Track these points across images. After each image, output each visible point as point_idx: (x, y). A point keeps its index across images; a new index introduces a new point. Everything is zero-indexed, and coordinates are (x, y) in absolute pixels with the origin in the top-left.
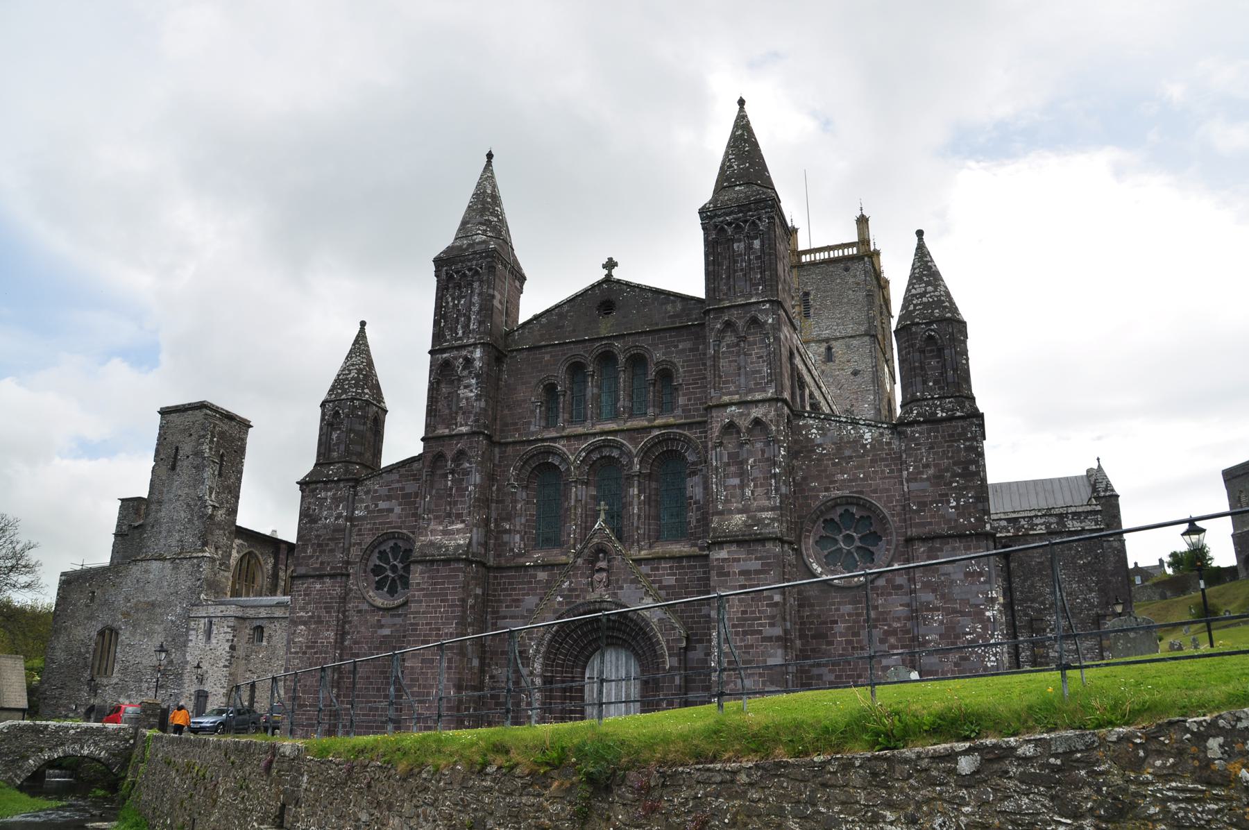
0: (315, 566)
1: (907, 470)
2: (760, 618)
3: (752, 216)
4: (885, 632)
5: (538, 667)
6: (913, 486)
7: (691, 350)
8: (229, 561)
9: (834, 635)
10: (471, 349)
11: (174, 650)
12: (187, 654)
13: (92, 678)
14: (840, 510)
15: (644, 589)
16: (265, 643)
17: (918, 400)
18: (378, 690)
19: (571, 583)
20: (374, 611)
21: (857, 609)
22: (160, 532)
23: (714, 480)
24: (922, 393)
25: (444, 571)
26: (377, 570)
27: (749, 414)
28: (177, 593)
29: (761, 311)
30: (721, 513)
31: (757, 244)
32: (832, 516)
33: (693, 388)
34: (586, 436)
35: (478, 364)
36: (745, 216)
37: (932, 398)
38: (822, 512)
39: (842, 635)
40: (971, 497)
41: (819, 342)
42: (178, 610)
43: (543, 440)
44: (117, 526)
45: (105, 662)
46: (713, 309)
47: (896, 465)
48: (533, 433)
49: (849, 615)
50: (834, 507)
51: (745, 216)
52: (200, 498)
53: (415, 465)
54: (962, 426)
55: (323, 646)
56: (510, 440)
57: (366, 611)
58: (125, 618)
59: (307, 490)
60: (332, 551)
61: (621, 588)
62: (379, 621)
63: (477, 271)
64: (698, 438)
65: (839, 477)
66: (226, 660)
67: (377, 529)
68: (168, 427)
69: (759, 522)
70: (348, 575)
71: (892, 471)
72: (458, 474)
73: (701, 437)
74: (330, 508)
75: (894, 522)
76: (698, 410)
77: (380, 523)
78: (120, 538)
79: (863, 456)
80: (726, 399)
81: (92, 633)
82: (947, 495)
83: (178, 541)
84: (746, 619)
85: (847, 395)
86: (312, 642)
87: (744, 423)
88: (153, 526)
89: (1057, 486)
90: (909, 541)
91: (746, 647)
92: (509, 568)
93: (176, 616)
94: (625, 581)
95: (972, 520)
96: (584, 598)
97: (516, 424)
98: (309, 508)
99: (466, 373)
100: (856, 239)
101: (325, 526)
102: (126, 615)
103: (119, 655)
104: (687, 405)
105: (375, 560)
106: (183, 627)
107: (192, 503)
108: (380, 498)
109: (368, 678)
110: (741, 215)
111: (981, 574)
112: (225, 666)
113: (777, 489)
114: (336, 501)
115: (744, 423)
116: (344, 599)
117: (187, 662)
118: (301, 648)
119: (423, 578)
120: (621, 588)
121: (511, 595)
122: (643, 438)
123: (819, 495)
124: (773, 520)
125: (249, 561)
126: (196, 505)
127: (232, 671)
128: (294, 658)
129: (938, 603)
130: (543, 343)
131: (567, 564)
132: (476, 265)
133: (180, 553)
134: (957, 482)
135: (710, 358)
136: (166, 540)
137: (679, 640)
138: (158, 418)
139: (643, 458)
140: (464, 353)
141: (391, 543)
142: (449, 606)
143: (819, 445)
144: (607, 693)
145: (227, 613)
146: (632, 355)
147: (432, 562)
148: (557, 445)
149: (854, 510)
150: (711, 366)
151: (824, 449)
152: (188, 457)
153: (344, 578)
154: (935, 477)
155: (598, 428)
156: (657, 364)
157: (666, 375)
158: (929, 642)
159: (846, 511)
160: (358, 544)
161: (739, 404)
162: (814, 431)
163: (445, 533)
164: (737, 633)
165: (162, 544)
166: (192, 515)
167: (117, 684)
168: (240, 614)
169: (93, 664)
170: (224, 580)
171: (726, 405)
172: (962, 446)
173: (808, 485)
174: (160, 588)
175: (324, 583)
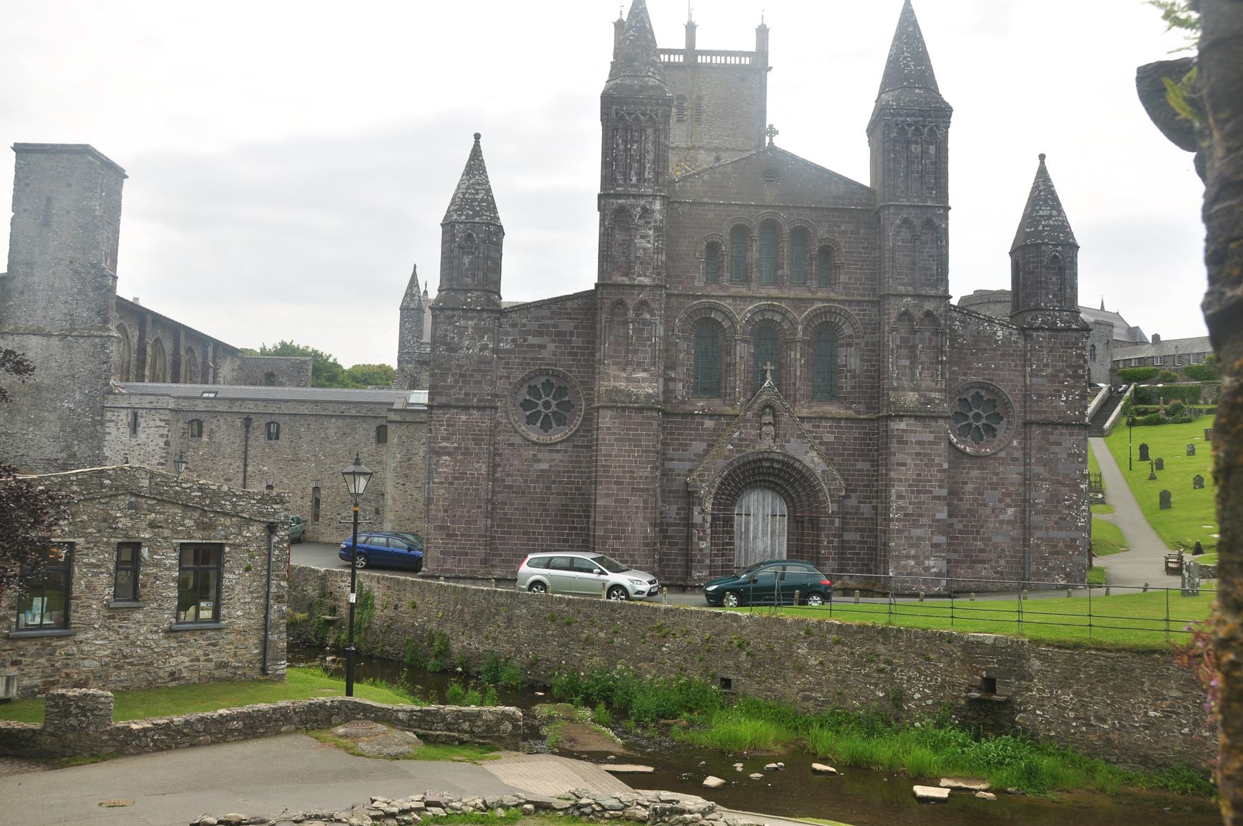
0: (458, 396)
1: (1031, 366)
2: (931, 481)
3: (931, 122)
4: (1003, 493)
5: (708, 506)
6: (1035, 380)
7: (852, 233)
9: (964, 493)
10: (650, 199)
12: (105, 449)
14: (972, 392)
15: (809, 445)
16: (205, 439)
17: (1043, 309)
18: (537, 521)
19: (741, 433)
20: (528, 445)
21: (982, 474)
22: (35, 301)
23: (890, 360)
24: (1046, 304)
25: (637, 418)
26: (526, 405)
27: (922, 307)
28: (73, 376)
29: (936, 215)
30: (896, 389)
31: (932, 149)
32: (966, 397)
33: (854, 269)
34: (753, 299)
35: (658, 216)
36: (924, 120)
37: (1054, 310)
38: (959, 392)
39: (970, 493)
40: (1077, 395)
41: (709, 150)
42: (78, 396)
43: (708, 297)
46: (894, 205)
47: (1020, 360)
48: (698, 288)
49: (976, 478)
50: (968, 389)
51: (924, 120)
53: (569, 304)
54: (1076, 337)
55: (473, 478)
56: (676, 292)
57: (519, 445)
59: (442, 316)
60: (479, 382)
61: (789, 441)
62: (534, 455)
63: (651, 116)
64: (857, 315)
65: (975, 365)
66: (161, 457)
67: (529, 364)
69: (931, 401)
70: (496, 408)
71: (1016, 365)
72: (638, 323)
73: (860, 315)
74: (472, 338)
75: (1017, 407)
76: (857, 289)
77: (531, 359)
79: (995, 350)
80: (902, 289)
82: (1059, 391)
84: (920, 481)
86: (459, 473)
87: (918, 314)
88: (22, 293)
90: (1027, 424)
91: (919, 503)
92: (677, 415)
93: (75, 403)
94: (792, 435)
96: (754, 447)
97: (680, 276)
98: (446, 336)
99: (642, 222)
100: (753, 48)
101: (467, 357)
104: (848, 284)
105: (524, 394)
108: (529, 332)
109: (525, 509)
110: (921, 119)
111: (1079, 456)
113: (943, 375)
114: (480, 332)
115: (918, 314)
116: (493, 432)
118: (446, 478)
119: (614, 423)
120: (789, 441)
121: (678, 439)
122: (806, 308)
124: (941, 400)
126: (89, 273)
128: (438, 488)
129: (1046, 475)
130: (706, 200)
131: (738, 416)
132: (651, 111)
134: (1068, 381)
135: (888, 250)
137: (840, 490)
140: (643, 202)
141: (543, 379)
142: (643, 451)
143: (961, 336)
144: (754, 527)
145: (159, 405)
146: (796, 227)
147: (624, 409)
148: (722, 303)
149: (983, 393)
150: (889, 258)
151: (964, 340)
152: (68, 212)
153: (493, 410)
154: (1052, 375)
155: (763, 292)
156: (821, 240)
157: (826, 252)
158: (1038, 504)
159: (977, 393)
160: (505, 377)
161: (915, 296)
162: (957, 323)
163: (629, 380)
164: (912, 492)
171: (902, 296)
175: (471, 415)
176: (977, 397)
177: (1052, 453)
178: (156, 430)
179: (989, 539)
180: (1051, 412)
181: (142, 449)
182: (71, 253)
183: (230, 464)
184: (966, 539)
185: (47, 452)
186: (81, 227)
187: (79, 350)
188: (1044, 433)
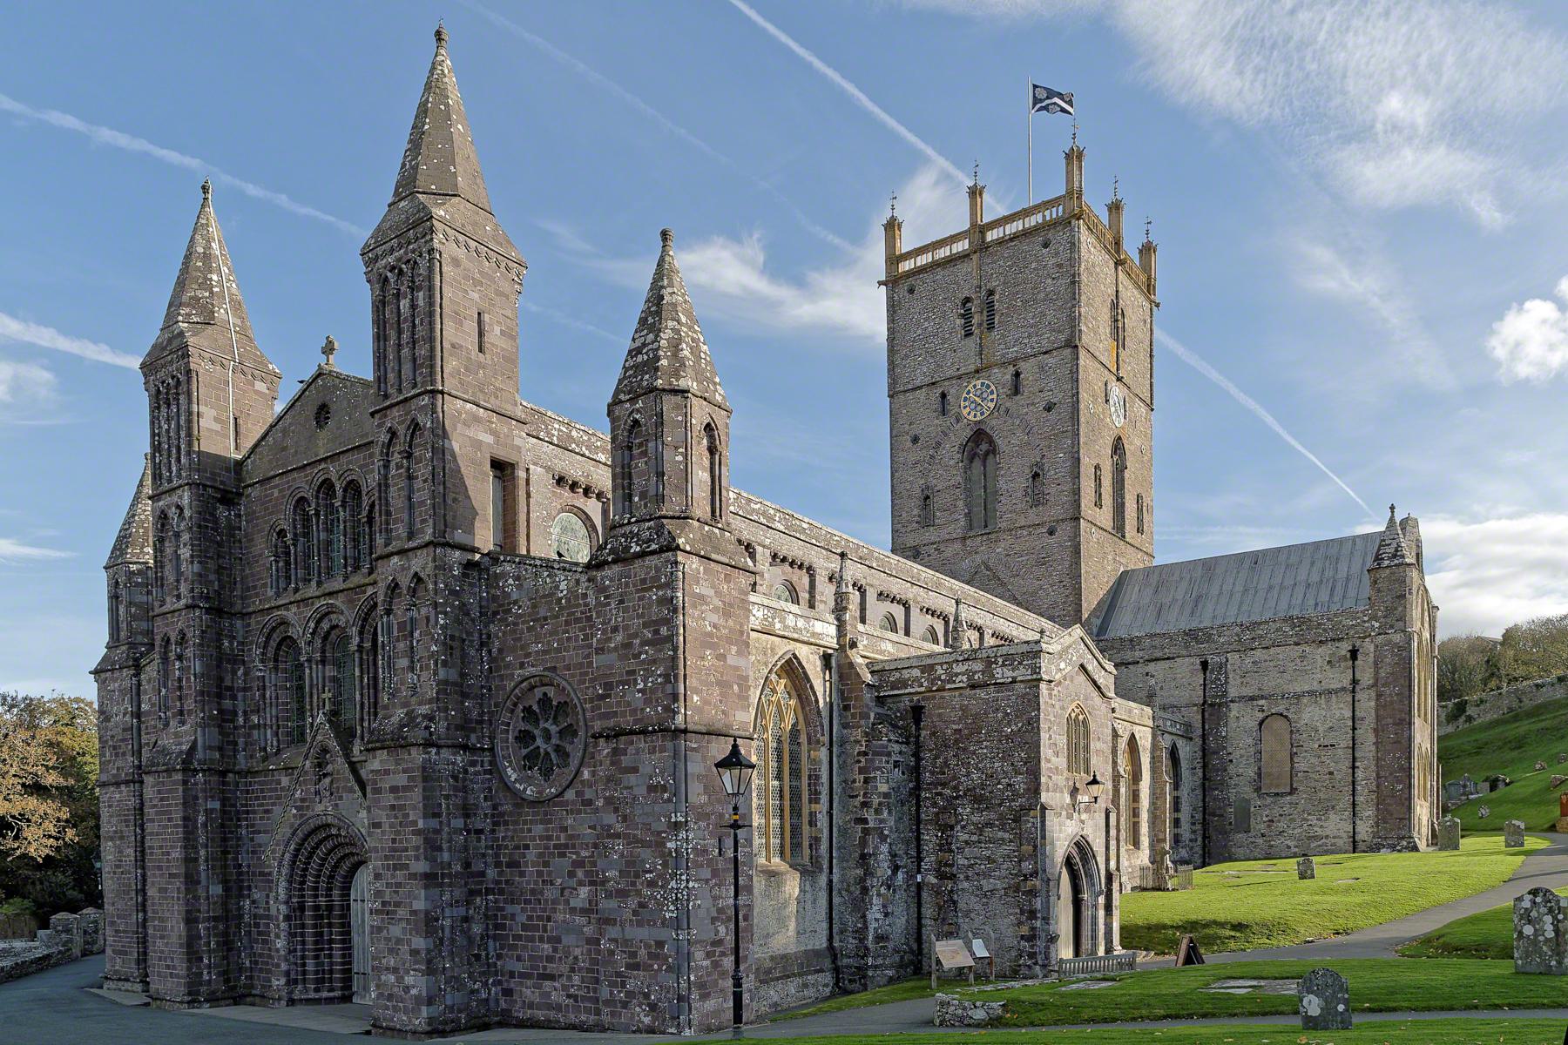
4: (574, 862)
14: (538, 693)
40: (660, 676)
85: (1037, 442)
89: (1348, 546)
95: (659, 708)
111: (664, 789)
123: (513, 674)
129: (619, 827)
134: (647, 653)
139: (363, 627)
143: (515, 602)
149: (551, 694)
151: (520, 607)
159: (545, 694)
172: (654, 597)
173: (503, 659)
176: (544, 701)
177: (626, 788)
179: (559, 940)
180: (624, 714)
184: (532, 939)
188: (615, 751)
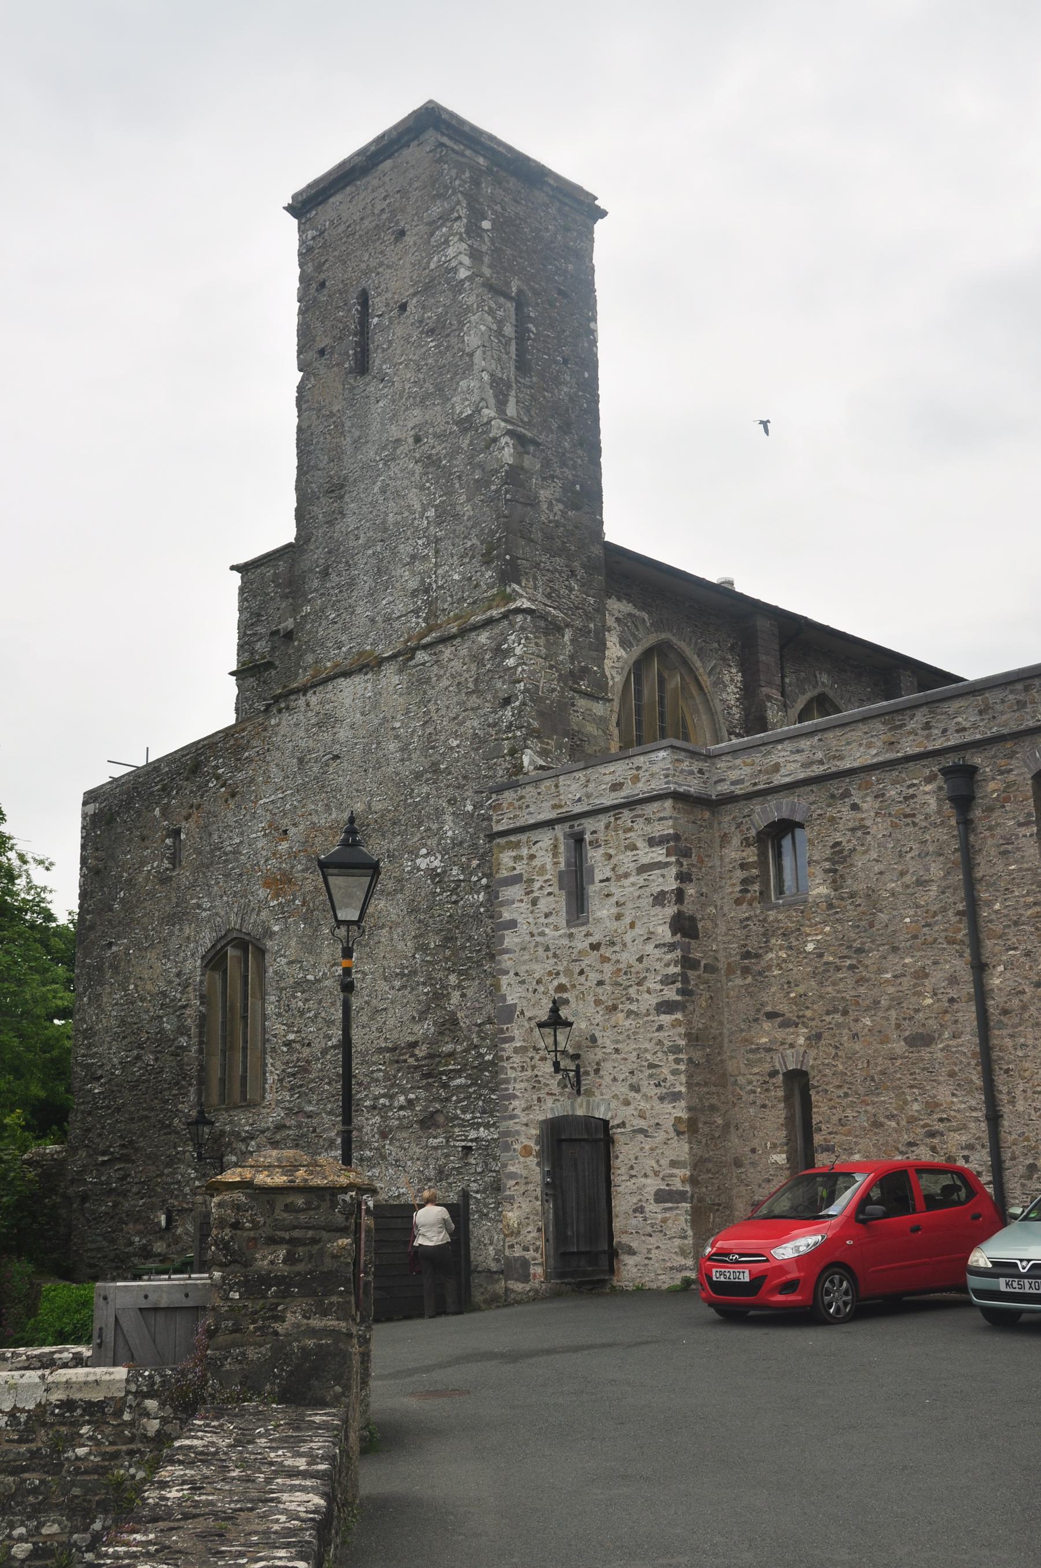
8: (601, 666)
11: (453, 979)
12: (504, 980)
13: (201, 1113)
28: (434, 768)
42: (450, 829)
44: (241, 647)
45: (240, 1056)
52: (466, 424)
58: (277, 896)
66: (667, 981)
68: (324, 246)
78: (251, 681)
81: (189, 965)
83: (414, 593)
88: (325, 574)
93: (444, 851)
102: (280, 882)
103: (275, 1027)
106: (473, 889)
107: (440, 449)
112: (666, 1007)
117: (508, 1013)
125: (662, 682)
126: (457, 450)
127: (699, 1023)
133: (430, 630)
136: (375, 603)
138: (292, 223)
145: (641, 789)
152: (403, 307)
165: (363, 620)
166: (449, 492)
167: (280, 1127)
168: (693, 786)
169: (202, 1068)
170: (591, 729)
174: (378, 767)
178: (640, 880)
181: (605, 960)
182: (416, 416)
183: (921, 974)
185: (391, 1022)
186: (432, 331)
187: (445, 682)
